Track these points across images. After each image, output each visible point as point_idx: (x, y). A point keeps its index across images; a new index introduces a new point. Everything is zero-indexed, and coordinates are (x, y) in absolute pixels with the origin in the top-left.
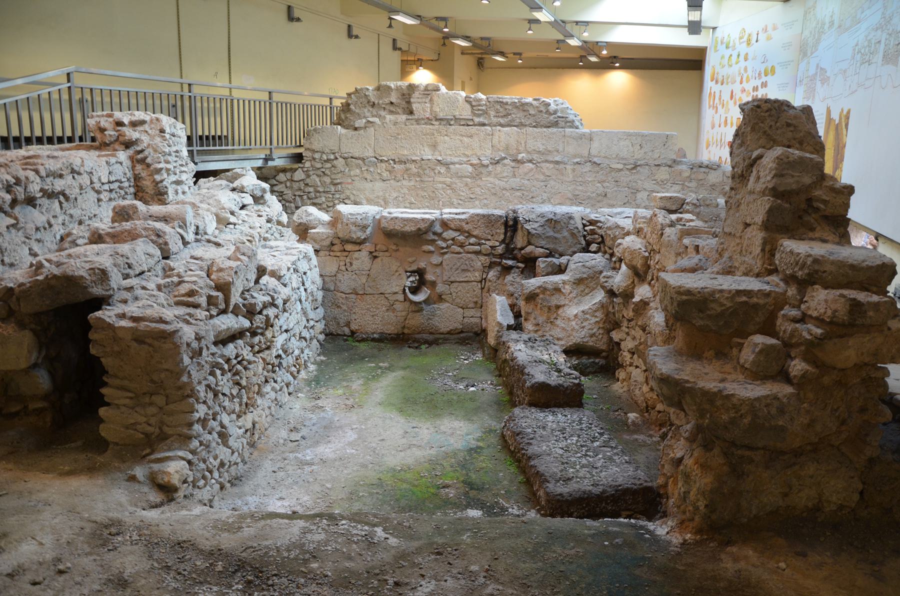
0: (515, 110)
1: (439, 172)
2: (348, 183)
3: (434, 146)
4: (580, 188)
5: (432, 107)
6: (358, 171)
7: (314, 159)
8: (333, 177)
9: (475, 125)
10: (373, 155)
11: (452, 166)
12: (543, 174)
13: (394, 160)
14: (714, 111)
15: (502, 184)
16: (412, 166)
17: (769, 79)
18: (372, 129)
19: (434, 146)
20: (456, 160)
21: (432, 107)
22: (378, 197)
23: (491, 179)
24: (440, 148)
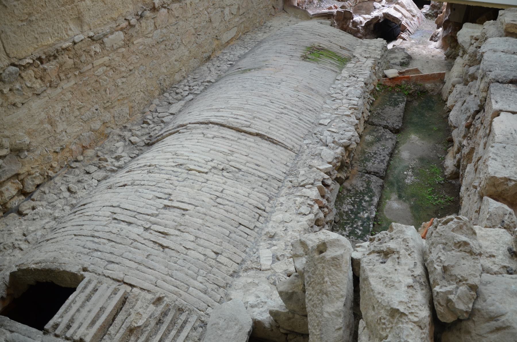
3: (79, 19)
4: (197, 20)
12: (174, 16)
13: (40, 59)
15: (148, 41)
16: (66, 58)
19: (79, 19)
20: (107, 29)
22: (41, 122)
23: (140, 40)
24: (87, 19)
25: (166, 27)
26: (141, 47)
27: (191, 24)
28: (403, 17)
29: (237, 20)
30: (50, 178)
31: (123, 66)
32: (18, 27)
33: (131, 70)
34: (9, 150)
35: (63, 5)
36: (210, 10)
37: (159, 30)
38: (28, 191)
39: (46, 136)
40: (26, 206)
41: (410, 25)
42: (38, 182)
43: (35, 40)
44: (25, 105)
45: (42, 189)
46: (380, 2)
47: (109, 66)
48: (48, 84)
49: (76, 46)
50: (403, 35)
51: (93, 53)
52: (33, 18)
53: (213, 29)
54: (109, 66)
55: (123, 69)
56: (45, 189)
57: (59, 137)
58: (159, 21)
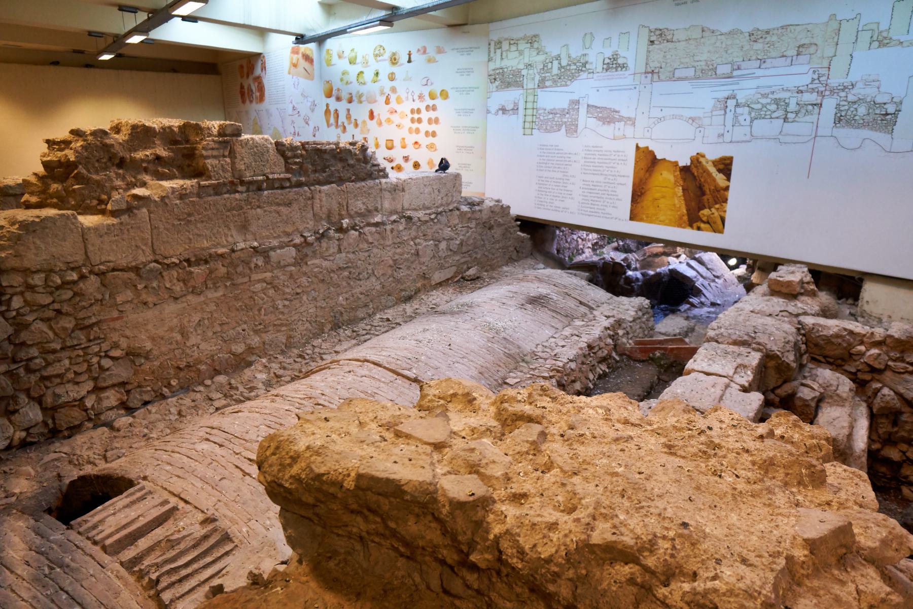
0: (333, 162)
1: (257, 266)
2: (114, 320)
4: (398, 250)
5: (233, 163)
6: (129, 294)
7: (31, 288)
8: (81, 315)
9: (291, 187)
10: (151, 258)
11: (272, 253)
12: (367, 241)
13: (188, 260)
14: (339, 130)
17: (438, 102)
18: (145, 210)
20: (275, 243)
21: (233, 163)
22: (171, 329)
23: (317, 261)
24: (253, 228)
25: (353, 253)
26: (316, 270)
27: (390, 254)
28: (699, 277)
29: (457, 258)
30: (164, 397)
31: (288, 287)
32: (173, 225)
33: (298, 294)
34: (124, 352)
35: (229, 211)
36: (418, 241)
37: (344, 255)
38: (131, 405)
39: (172, 347)
40: (124, 421)
41: (709, 288)
42: (146, 398)
43: (187, 241)
44: (158, 306)
45: (149, 407)
46: (678, 257)
47: (271, 283)
48: (190, 290)
49: (233, 255)
50: (694, 300)
51: (253, 266)
52: (192, 219)
53: (420, 263)
54: (271, 283)
55: (287, 290)
56: (153, 408)
57: (188, 351)
58: (345, 244)
